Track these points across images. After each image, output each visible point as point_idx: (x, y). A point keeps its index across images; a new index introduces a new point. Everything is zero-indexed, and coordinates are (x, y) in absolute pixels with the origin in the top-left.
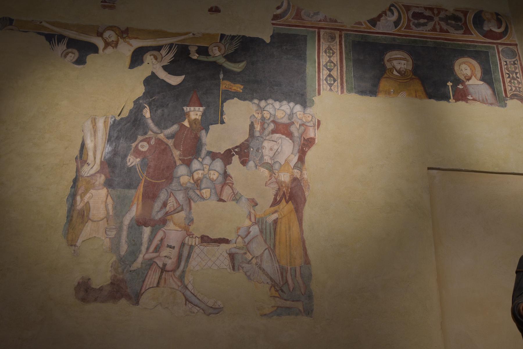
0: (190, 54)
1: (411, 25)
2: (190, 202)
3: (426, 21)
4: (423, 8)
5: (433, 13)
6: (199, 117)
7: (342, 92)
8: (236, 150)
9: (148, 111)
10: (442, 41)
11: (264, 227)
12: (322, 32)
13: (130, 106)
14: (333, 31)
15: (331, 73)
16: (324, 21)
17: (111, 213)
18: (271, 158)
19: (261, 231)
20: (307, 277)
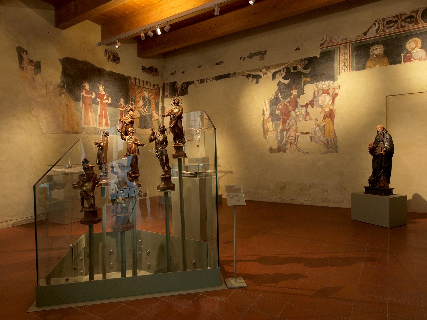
0: (290, 70)
1: (385, 29)
2: (296, 122)
3: (393, 24)
4: (392, 17)
5: (398, 18)
6: (296, 94)
7: (349, 72)
8: (309, 103)
9: (280, 95)
10: (401, 33)
11: (321, 127)
12: (341, 46)
13: (275, 94)
14: (346, 44)
15: (345, 64)
16: (342, 40)
17: (274, 129)
18: (322, 103)
19: (320, 129)
20: (336, 141)
